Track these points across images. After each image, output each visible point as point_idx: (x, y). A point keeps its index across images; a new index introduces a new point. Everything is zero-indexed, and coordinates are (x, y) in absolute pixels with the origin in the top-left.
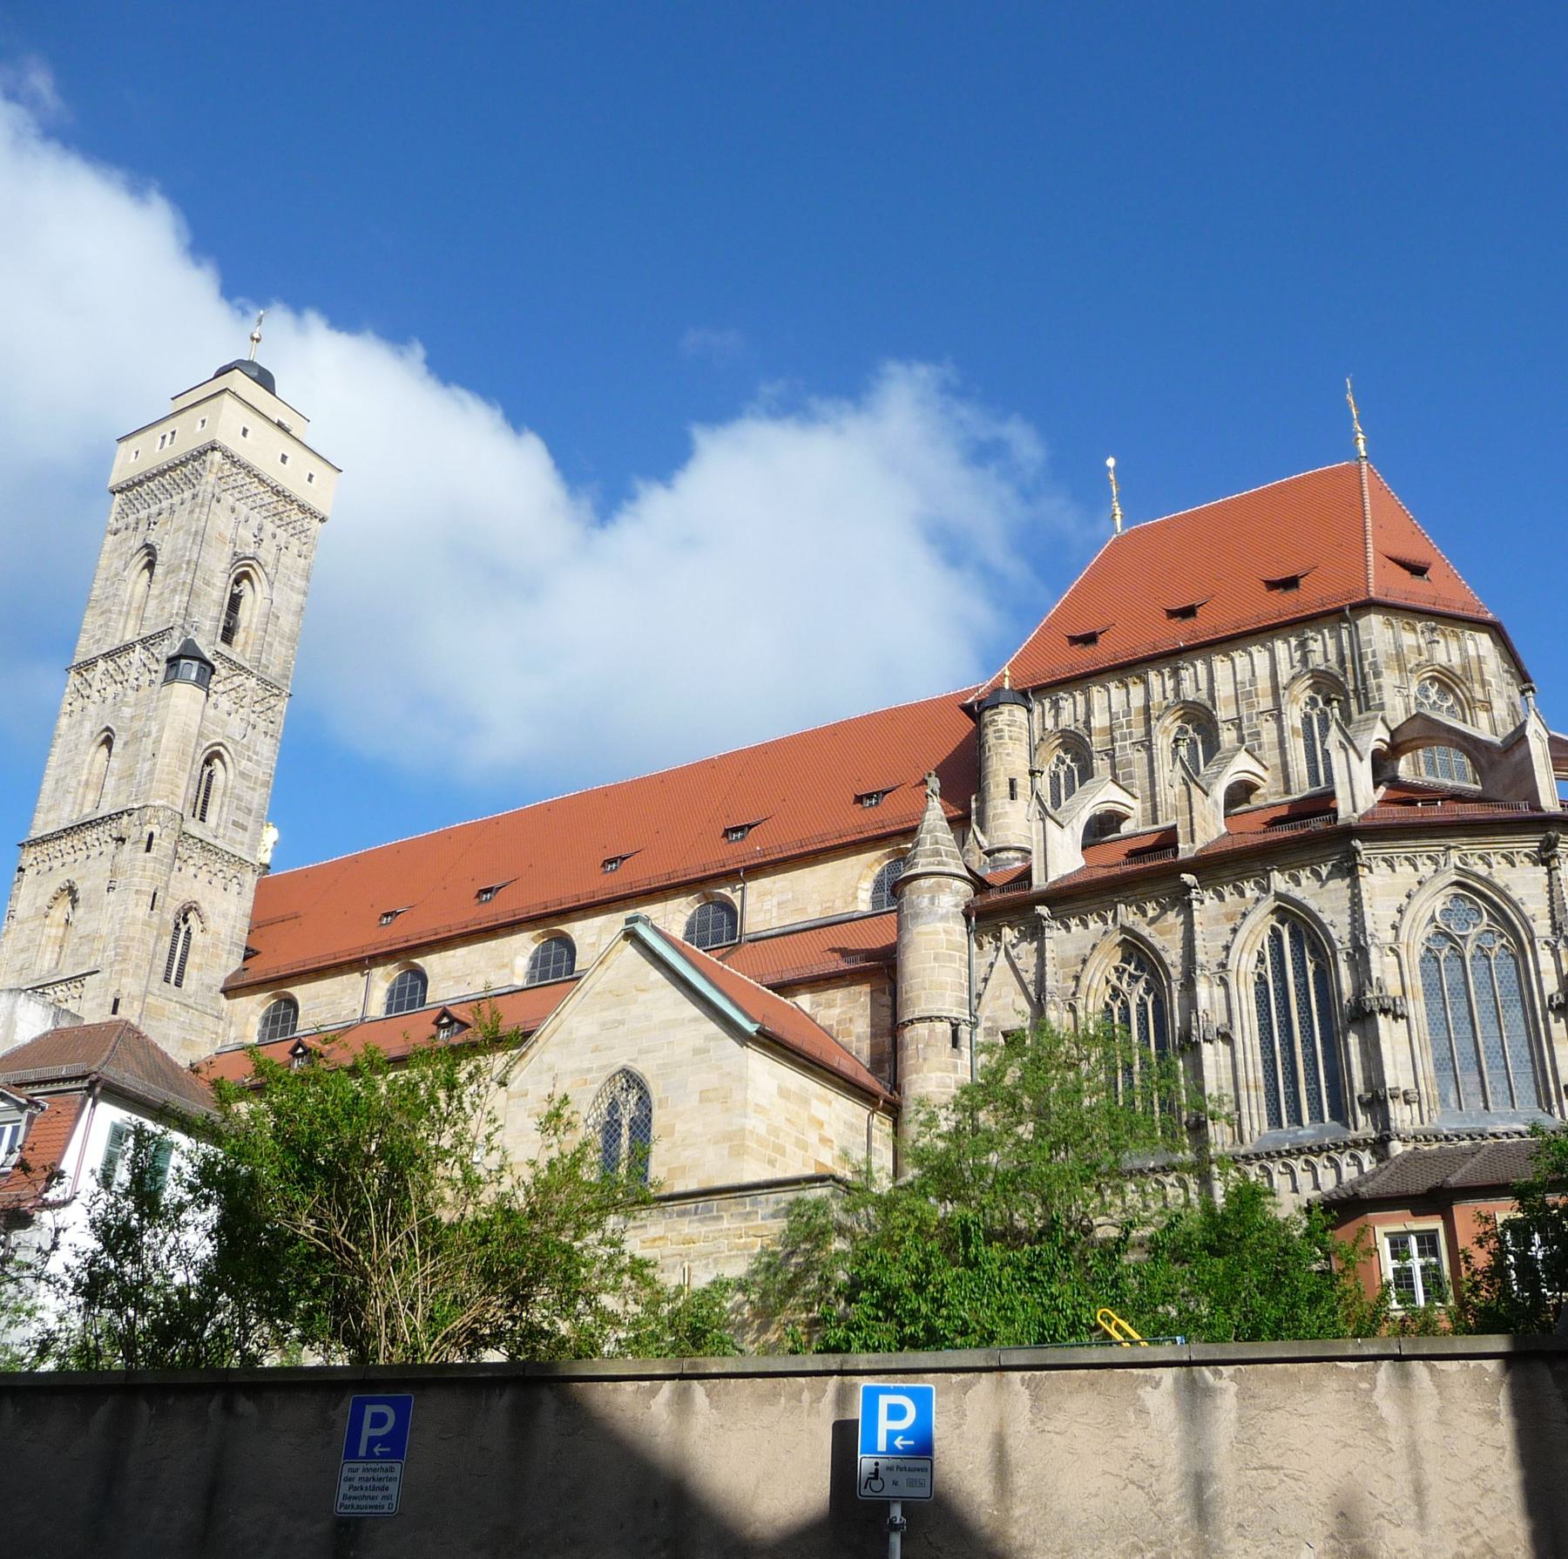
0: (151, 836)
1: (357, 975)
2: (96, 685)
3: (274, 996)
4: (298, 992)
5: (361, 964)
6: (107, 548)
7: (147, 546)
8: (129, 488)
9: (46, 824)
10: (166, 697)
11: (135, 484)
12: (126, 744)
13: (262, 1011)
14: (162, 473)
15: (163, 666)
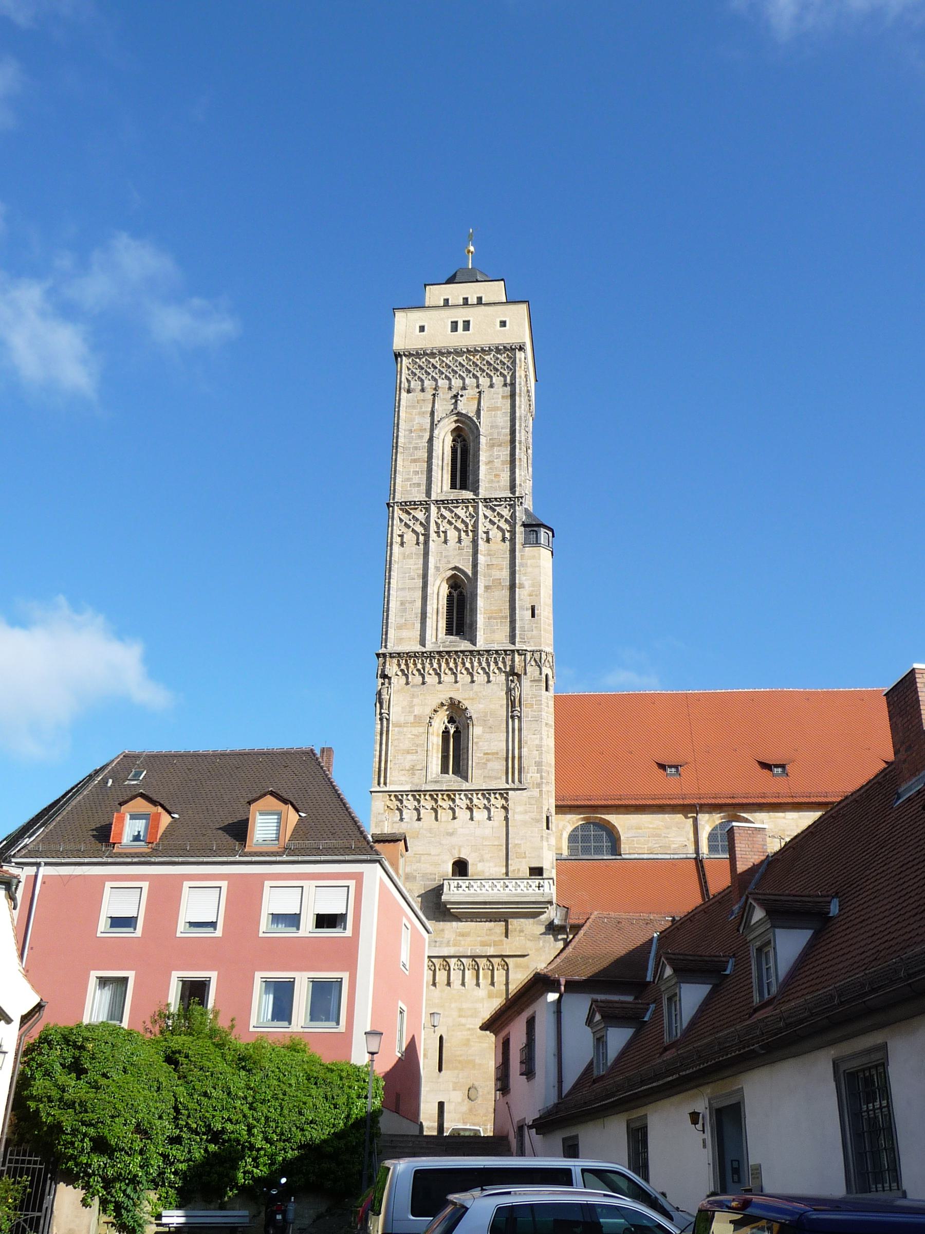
0: (547, 676)
1: (680, 816)
2: (433, 527)
3: (583, 819)
4: (614, 819)
5: (689, 809)
6: (403, 403)
7: (458, 414)
8: (418, 355)
9: (400, 640)
10: (534, 557)
11: (425, 354)
12: (487, 588)
13: (570, 829)
14: (459, 353)
15: (519, 529)
